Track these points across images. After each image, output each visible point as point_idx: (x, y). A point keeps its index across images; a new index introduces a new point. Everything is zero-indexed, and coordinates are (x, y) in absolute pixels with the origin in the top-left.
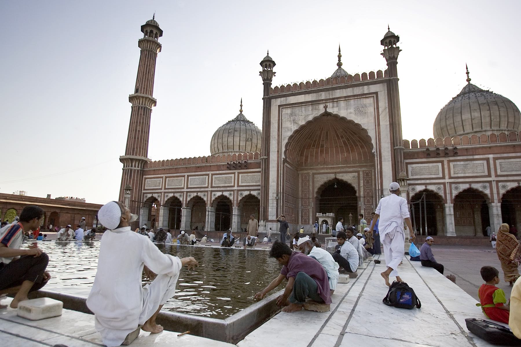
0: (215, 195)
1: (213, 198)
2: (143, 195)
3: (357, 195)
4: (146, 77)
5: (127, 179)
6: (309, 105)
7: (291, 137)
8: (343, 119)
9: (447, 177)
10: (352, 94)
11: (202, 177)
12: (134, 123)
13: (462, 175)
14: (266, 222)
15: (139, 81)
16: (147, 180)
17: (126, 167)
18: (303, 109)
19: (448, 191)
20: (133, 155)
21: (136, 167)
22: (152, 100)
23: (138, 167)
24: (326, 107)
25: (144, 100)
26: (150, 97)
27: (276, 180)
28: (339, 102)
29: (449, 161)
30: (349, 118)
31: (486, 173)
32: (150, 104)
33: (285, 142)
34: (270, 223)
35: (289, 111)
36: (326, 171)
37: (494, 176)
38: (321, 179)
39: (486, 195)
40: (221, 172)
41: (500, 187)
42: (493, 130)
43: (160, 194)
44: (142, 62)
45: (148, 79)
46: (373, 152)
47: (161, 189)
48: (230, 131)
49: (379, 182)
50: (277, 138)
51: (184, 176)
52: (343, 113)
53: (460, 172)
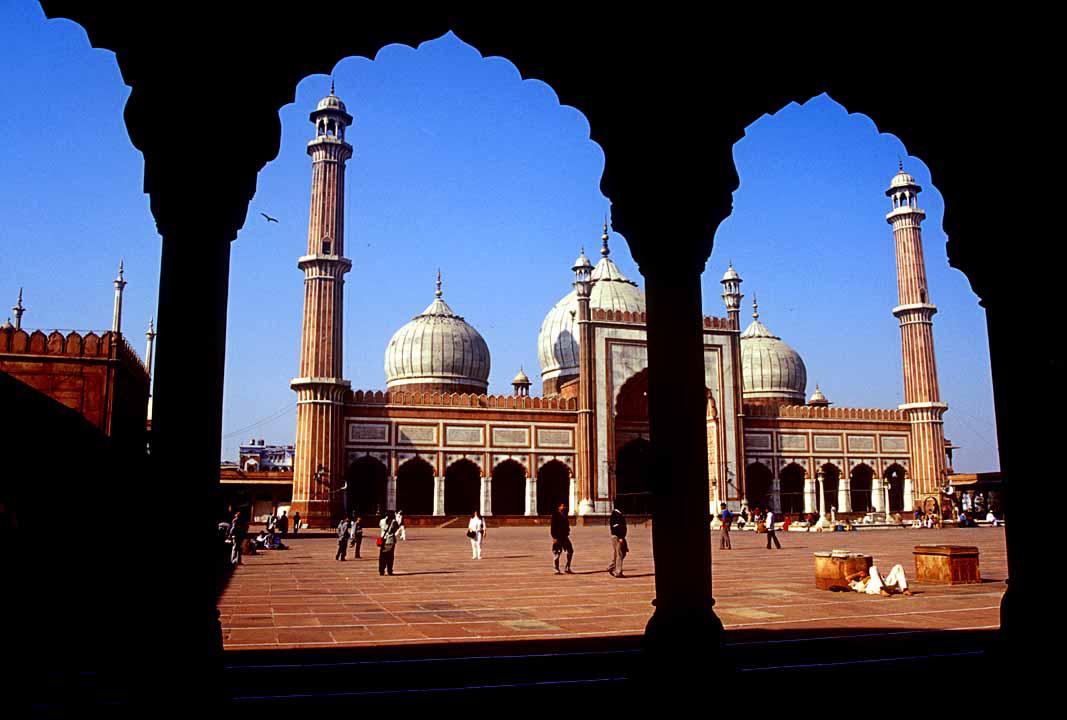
0: (497, 459)
7: (624, 388)
9: (775, 450)
15: (327, 226)
16: (351, 426)
17: (322, 399)
18: (638, 349)
22: (344, 264)
27: (606, 443)
33: (617, 392)
34: (601, 502)
36: (630, 428)
40: (506, 423)
43: (386, 454)
44: (329, 186)
48: (455, 339)
51: (437, 425)
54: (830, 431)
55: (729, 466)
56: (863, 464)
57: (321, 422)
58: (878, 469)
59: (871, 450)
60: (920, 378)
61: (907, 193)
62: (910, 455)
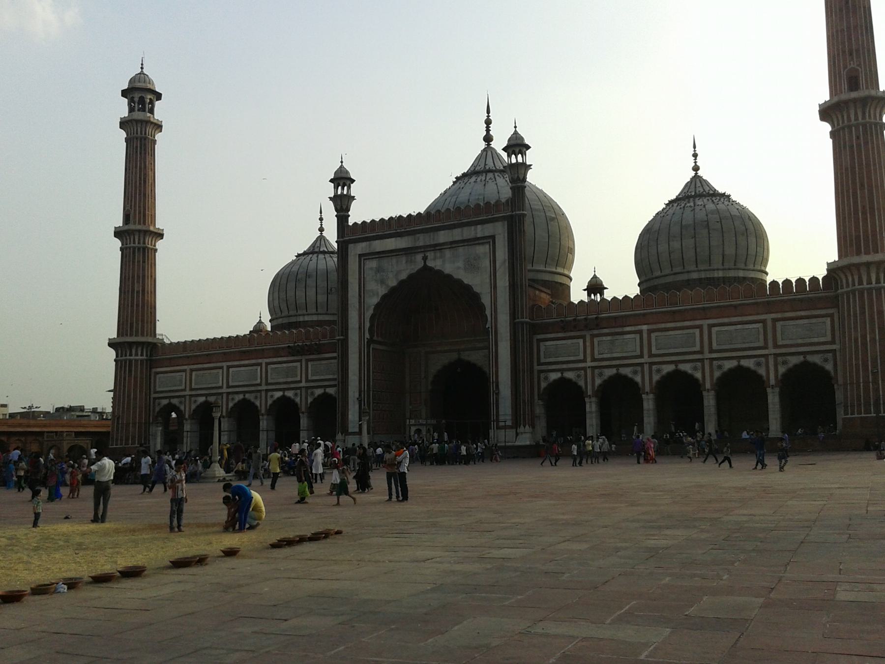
0: (272, 396)
1: (270, 402)
2: (154, 403)
4: (140, 191)
5: (125, 379)
7: (378, 306)
8: (449, 277)
9: (589, 359)
10: (460, 238)
11: (250, 368)
12: (129, 279)
13: (609, 356)
14: (346, 435)
16: (158, 376)
18: (394, 260)
19: (589, 380)
20: (131, 335)
21: (139, 356)
23: (142, 355)
24: (425, 259)
25: (142, 235)
26: (152, 228)
28: (443, 250)
29: (593, 336)
30: (456, 277)
31: (638, 353)
32: (152, 241)
33: (369, 313)
34: (350, 436)
35: (372, 264)
37: (647, 356)
38: (439, 361)
39: (636, 384)
40: (280, 359)
41: (654, 372)
43: (183, 399)
44: (129, 164)
45: (145, 195)
46: (487, 327)
47: (184, 390)
50: (358, 307)
51: (222, 368)
53: (606, 351)
54: (679, 324)
55: (501, 387)
56: (740, 368)
57: (121, 377)
58: (772, 374)
59: (756, 345)
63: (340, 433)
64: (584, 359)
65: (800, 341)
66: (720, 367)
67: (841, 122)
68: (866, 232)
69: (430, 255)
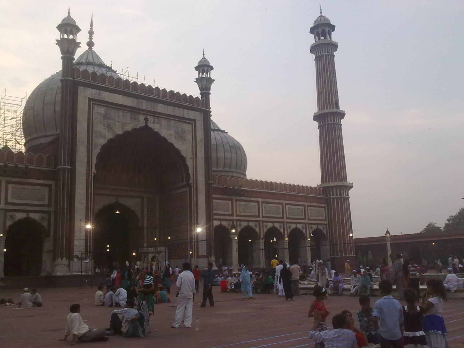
3: (140, 224)
6: (128, 111)
8: (164, 139)
18: (121, 113)
24: (147, 120)
28: (160, 118)
29: (237, 200)
30: (169, 141)
31: (257, 214)
33: (96, 151)
35: (102, 110)
36: (107, 192)
41: (264, 226)
42: (237, 173)
49: (195, 216)
50: (86, 143)
52: (164, 133)
53: (243, 211)
54: (274, 201)
56: (296, 228)
60: (334, 164)
61: (327, 29)
62: (327, 222)
63: (60, 258)
64: (232, 214)
65: (316, 218)
66: (290, 227)
67: (332, 121)
68: (343, 172)
69: (151, 119)
